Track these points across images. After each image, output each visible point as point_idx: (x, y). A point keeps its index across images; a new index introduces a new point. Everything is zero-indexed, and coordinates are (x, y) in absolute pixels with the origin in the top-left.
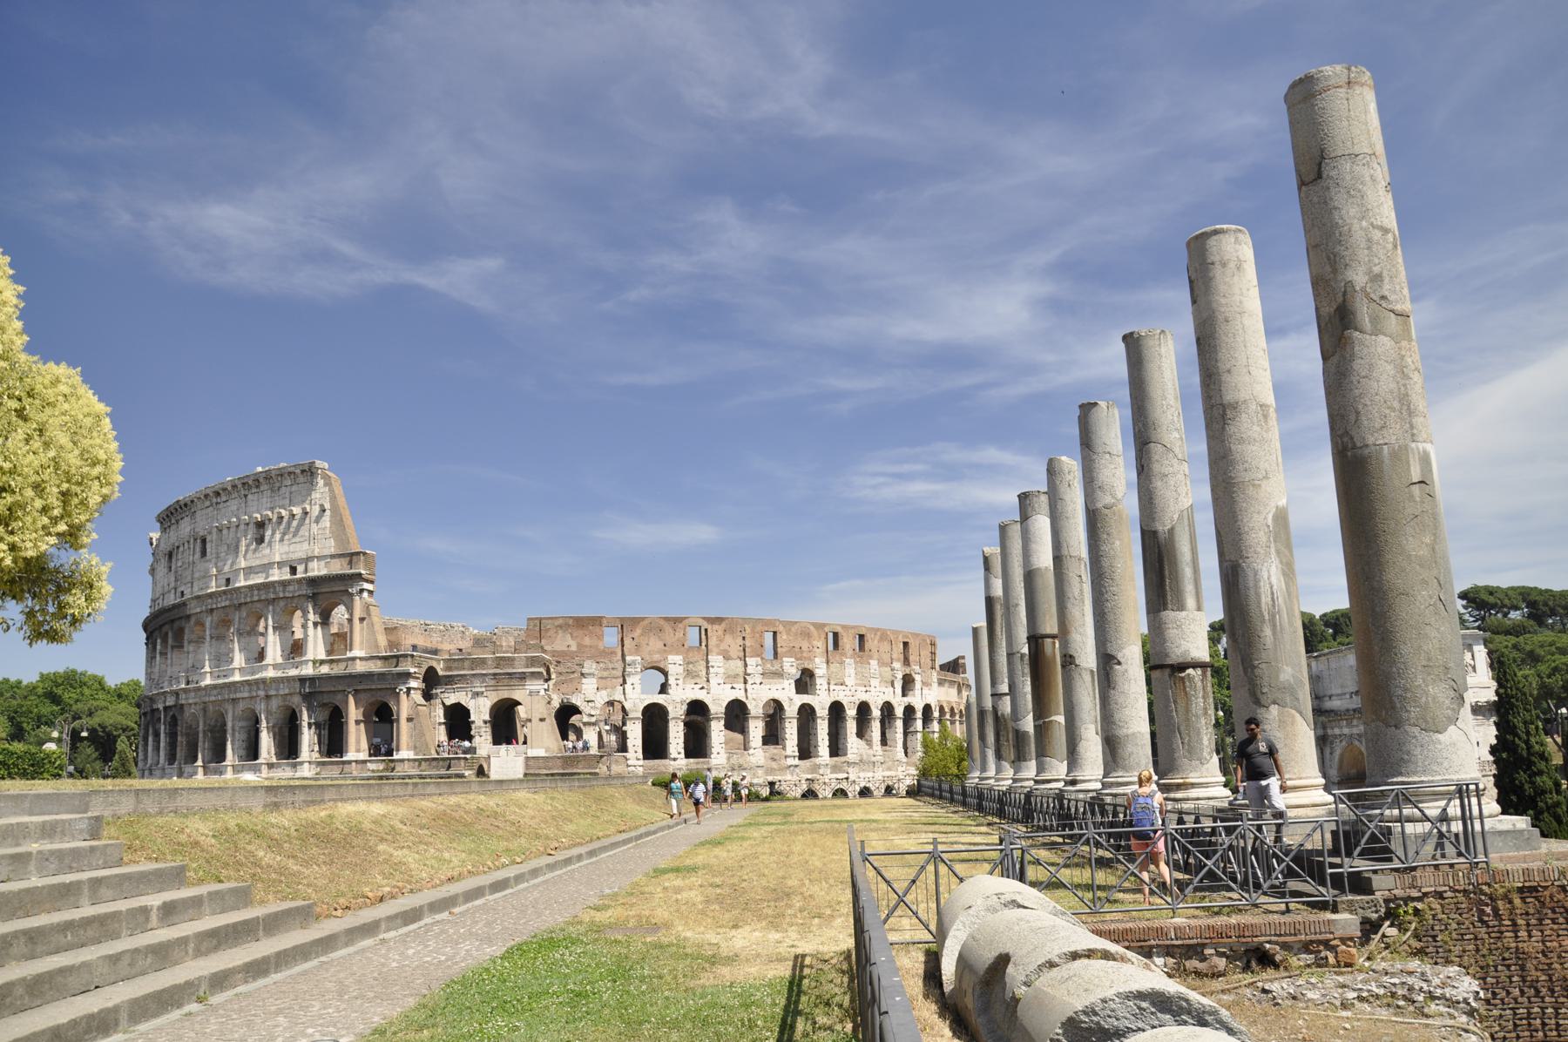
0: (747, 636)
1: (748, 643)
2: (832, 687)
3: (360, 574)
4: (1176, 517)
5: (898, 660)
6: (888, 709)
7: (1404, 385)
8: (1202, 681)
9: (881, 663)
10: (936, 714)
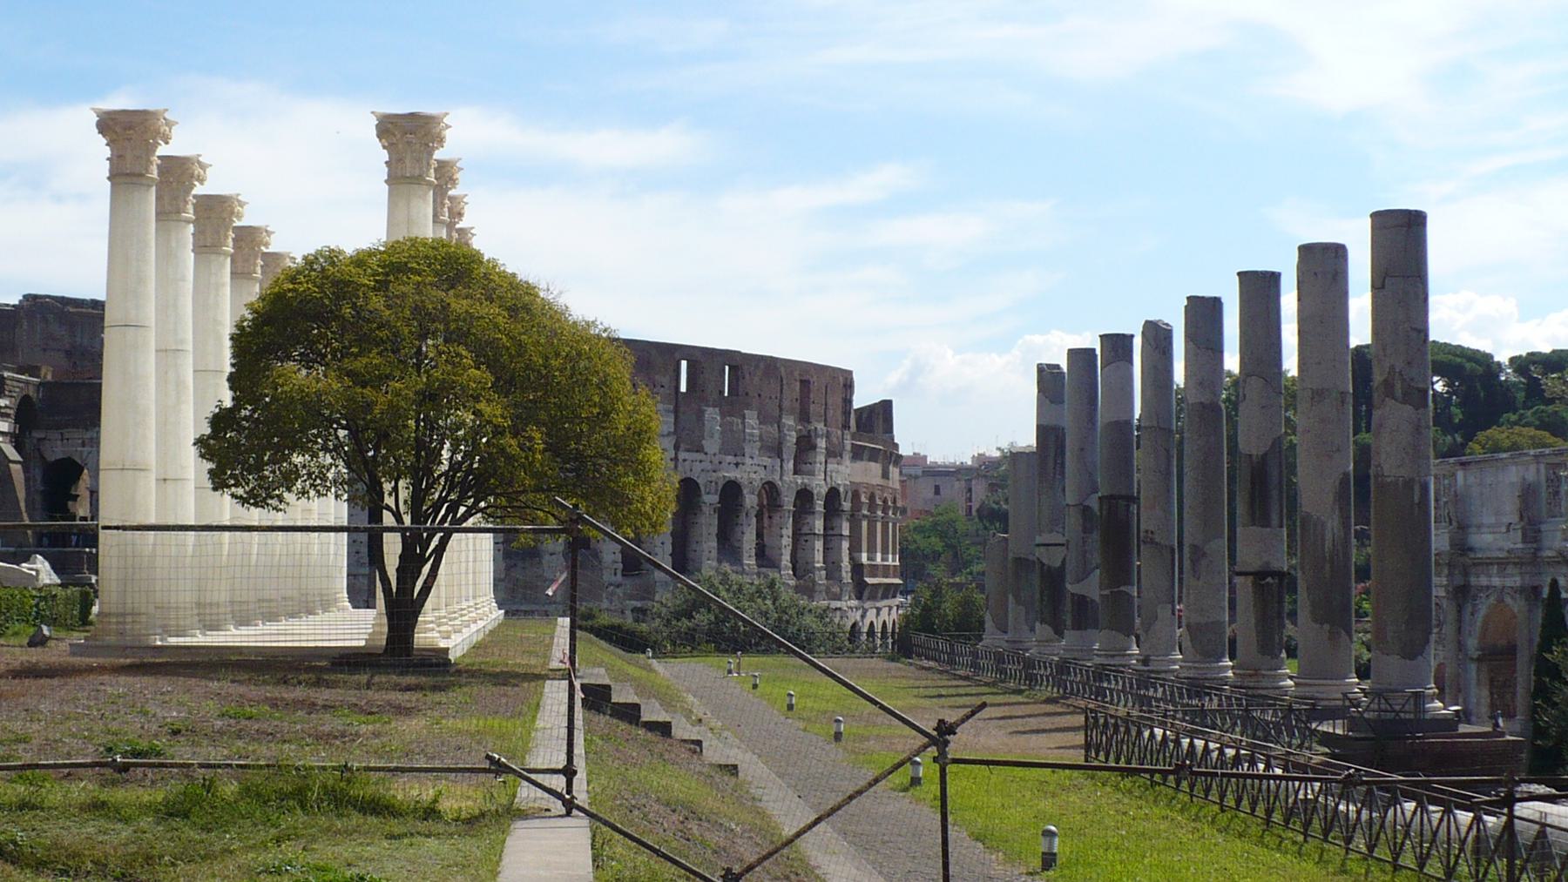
2: (682, 455)
5: (792, 412)
6: (771, 491)
9: (764, 419)
10: (847, 505)
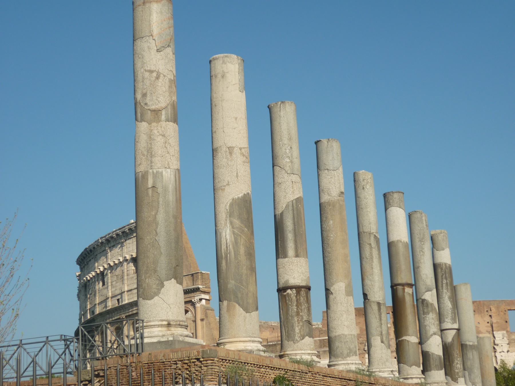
0: (493, 314)
1: (494, 320)
3: (199, 288)
4: (284, 206)
7: (151, 144)
8: (296, 297)
